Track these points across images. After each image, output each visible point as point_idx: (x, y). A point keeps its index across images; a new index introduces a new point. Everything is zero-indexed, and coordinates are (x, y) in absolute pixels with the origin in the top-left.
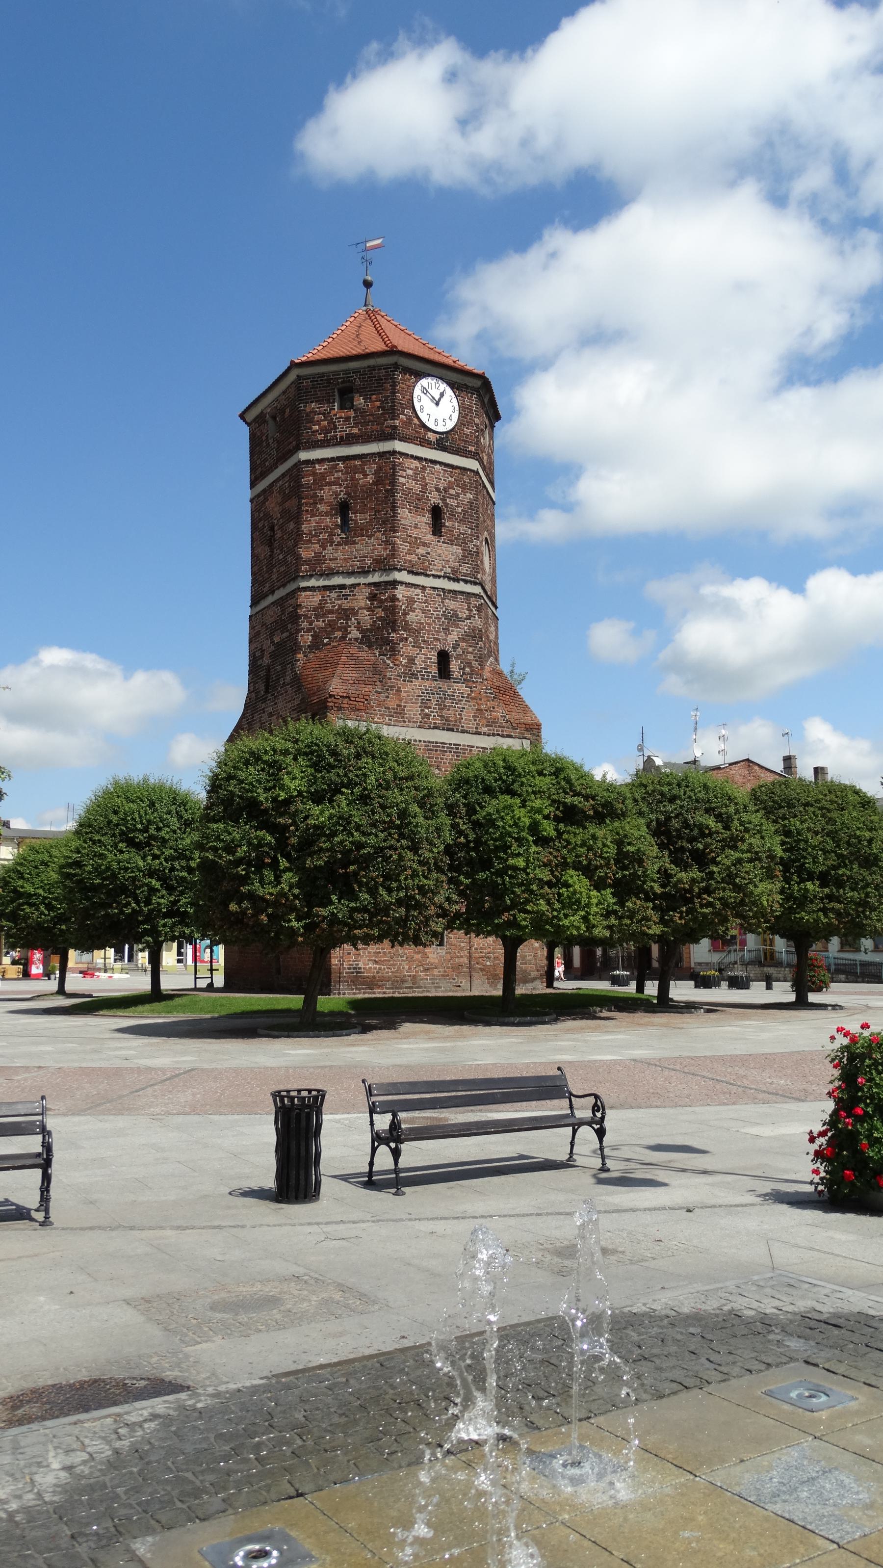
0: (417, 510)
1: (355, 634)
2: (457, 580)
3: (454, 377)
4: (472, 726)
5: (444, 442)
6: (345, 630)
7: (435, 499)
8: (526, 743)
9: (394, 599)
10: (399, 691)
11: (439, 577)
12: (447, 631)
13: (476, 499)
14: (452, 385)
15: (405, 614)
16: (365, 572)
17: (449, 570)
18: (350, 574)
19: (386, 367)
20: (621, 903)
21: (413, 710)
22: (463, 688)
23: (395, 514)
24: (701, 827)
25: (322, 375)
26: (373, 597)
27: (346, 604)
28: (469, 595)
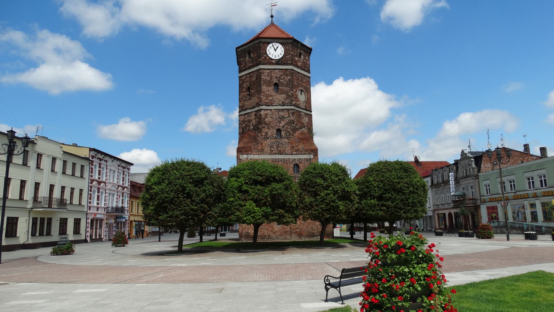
0: (269, 85)
1: (252, 127)
2: (284, 105)
4: (290, 152)
5: (278, 62)
6: (249, 126)
7: (275, 81)
8: (312, 156)
9: (260, 115)
10: (262, 144)
12: (280, 122)
13: (292, 78)
14: (281, 44)
15: (264, 119)
16: (254, 108)
18: (250, 109)
19: (258, 43)
20: (273, 210)
21: (267, 149)
22: (286, 140)
23: (261, 88)
24: (316, 183)
25: (243, 50)
26: (256, 115)
27: (249, 118)
28: (288, 110)
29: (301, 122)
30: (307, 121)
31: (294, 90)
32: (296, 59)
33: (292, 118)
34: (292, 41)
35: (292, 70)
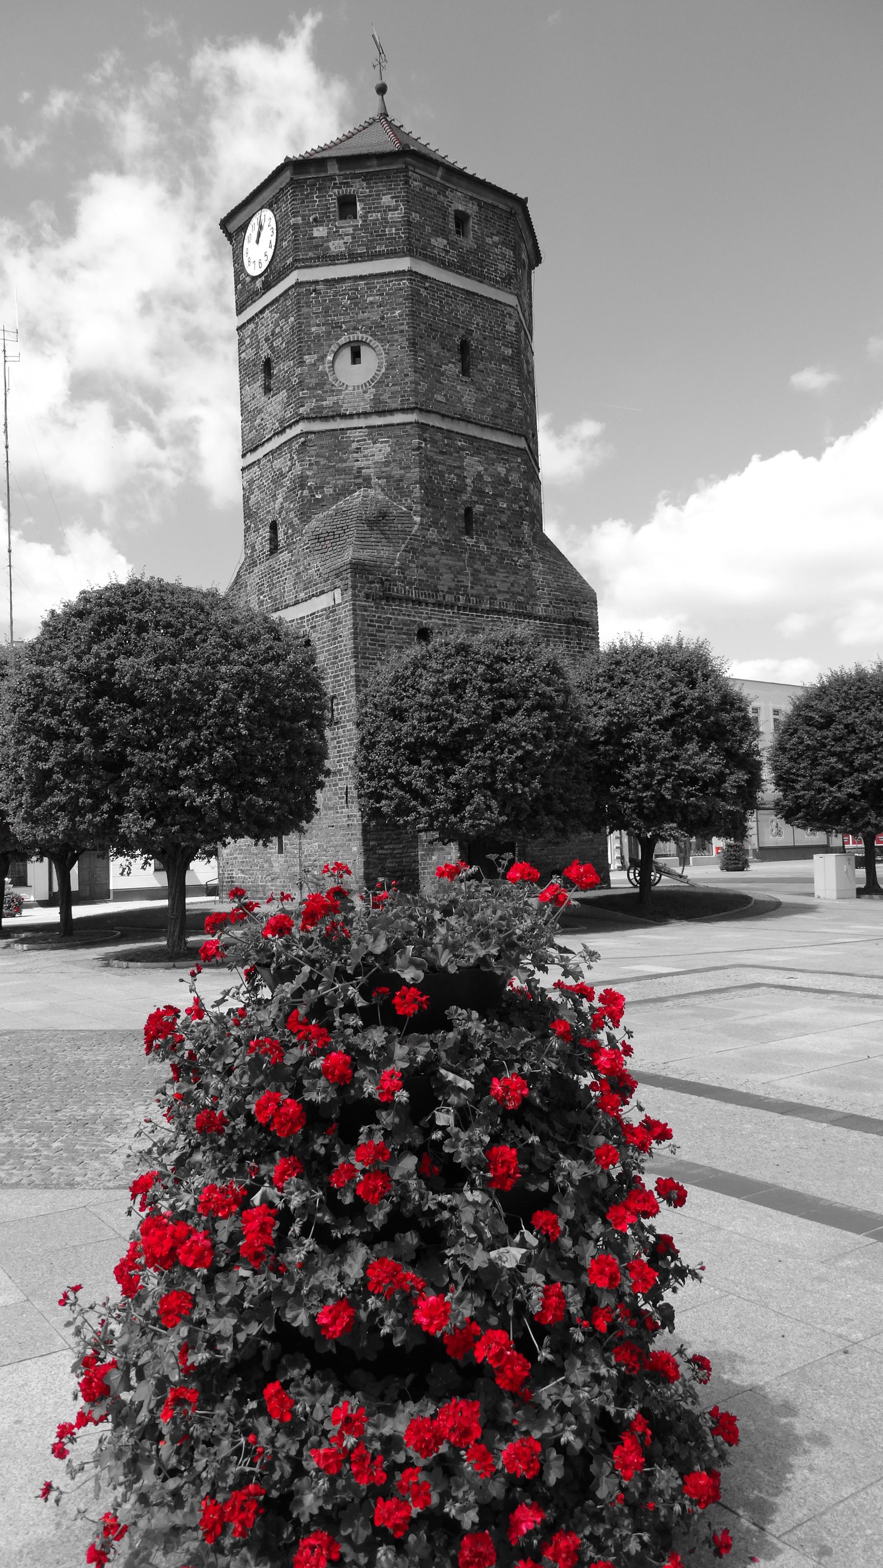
2: (283, 431)
3: (268, 194)
7: (265, 352)
11: (270, 439)
12: (274, 497)
29: (344, 471)
30: (380, 457)
31: (309, 359)
32: (319, 232)
33: (298, 469)
35: (298, 284)
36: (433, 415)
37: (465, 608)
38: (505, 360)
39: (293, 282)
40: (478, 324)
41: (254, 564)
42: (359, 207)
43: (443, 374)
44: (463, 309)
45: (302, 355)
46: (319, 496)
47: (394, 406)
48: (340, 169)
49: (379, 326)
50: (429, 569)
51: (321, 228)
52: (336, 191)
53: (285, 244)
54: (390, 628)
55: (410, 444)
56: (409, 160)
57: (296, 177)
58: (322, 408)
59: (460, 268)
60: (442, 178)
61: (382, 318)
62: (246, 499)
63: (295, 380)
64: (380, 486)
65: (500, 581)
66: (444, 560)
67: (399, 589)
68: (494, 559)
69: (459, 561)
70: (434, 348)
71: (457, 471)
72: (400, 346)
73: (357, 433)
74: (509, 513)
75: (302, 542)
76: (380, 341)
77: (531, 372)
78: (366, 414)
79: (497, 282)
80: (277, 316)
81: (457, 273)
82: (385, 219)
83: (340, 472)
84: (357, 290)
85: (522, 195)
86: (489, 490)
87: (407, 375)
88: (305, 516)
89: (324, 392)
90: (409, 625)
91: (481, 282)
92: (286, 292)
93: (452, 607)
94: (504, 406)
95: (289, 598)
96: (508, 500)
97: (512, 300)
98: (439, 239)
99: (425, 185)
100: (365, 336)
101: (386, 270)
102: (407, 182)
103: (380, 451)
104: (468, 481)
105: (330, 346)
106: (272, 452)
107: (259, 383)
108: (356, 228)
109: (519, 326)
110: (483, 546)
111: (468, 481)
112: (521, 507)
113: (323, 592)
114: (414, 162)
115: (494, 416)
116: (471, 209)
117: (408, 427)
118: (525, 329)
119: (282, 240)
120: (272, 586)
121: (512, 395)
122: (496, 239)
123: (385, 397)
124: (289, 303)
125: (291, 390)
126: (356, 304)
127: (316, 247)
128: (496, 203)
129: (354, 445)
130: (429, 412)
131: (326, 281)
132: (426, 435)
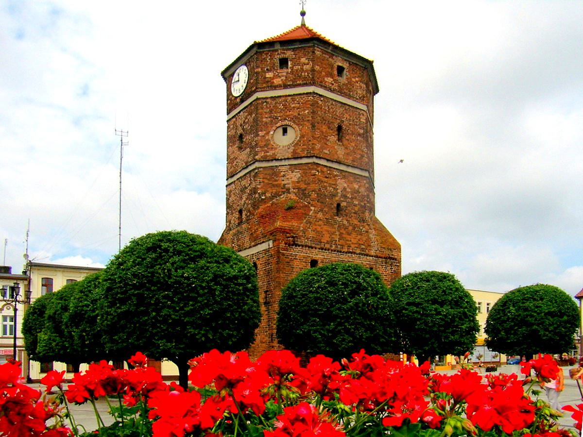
3: (245, 59)
11: (240, 171)
12: (241, 198)
17: (244, 164)
29: (277, 186)
32: (269, 75)
33: (253, 185)
34: (255, 49)
35: (258, 99)
36: (322, 159)
37: (335, 251)
38: (360, 135)
39: (255, 98)
40: (347, 118)
41: (231, 230)
42: (289, 63)
43: (328, 141)
44: (340, 110)
45: (257, 132)
46: (263, 197)
47: (303, 155)
48: (281, 46)
49: (296, 117)
50: (318, 231)
51: (270, 73)
52: (278, 56)
53: (252, 81)
54: (297, 259)
55: (310, 173)
56: (315, 42)
57: (259, 50)
58: (267, 156)
59: (338, 92)
60: (331, 51)
61: (299, 114)
62: (228, 200)
63: (254, 143)
64: (294, 192)
65: (353, 239)
66: (326, 228)
67: (303, 241)
68: (351, 228)
69: (333, 228)
70: (324, 128)
71: (334, 186)
72: (307, 127)
73: (284, 168)
74: (359, 207)
75: (255, 219)
76: (297, 125)
77: (372, 142)
78: (288, 159)
79: (357, 99)
80: (246, 114)
81: (338, 94)
82: (302, 69)
83: (274, 186)
84: (287, 101)
85: (370, 59)
86: (349, 195)
87: (310, 141)
88: (255, 206)
89: (268, 149)
90: (306, 258)
91: (349, 99)
92: (251, 103)
93: (328, 250)
94: (359, 156)
95: (247, 245)
96: (359, 200)
97: (364, 108)
98: (329, 78)
99: (323, 53)
100: (290, 123)
101: (302, 92)
102: (313, 52)
103: (296, 176)
104: (339, 191)
105: (272, 127)
106: (241, 177)
107: (236, 146)
108: (287, 73)
109: (367, 120)
110: (345, 222)
111: (339, 191)
112: (365, 204)
113: (263, 242)
114: (318, 43)
115: (353, 161)
116: (345, 65)
117: (310, 165)
118: (370, 122)
119: (251, 79)
120: (238, 240)
121: (363, 151)
122: (357, 79)
123: (299, 151)
124: (253, 108)
125: (252, 148)
126: (286, 108)
127: (268, 82)
128: (358, 63)
129: (282, 174)
130: (320, 158)
131: (272, 97)
132: (319, 169)
